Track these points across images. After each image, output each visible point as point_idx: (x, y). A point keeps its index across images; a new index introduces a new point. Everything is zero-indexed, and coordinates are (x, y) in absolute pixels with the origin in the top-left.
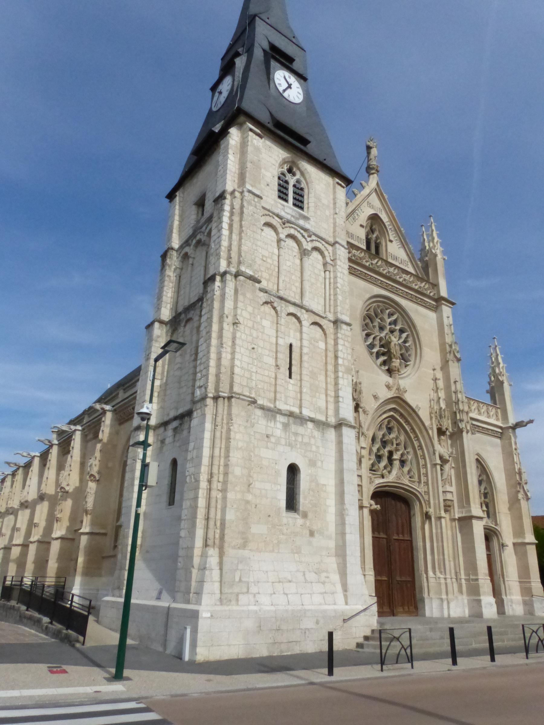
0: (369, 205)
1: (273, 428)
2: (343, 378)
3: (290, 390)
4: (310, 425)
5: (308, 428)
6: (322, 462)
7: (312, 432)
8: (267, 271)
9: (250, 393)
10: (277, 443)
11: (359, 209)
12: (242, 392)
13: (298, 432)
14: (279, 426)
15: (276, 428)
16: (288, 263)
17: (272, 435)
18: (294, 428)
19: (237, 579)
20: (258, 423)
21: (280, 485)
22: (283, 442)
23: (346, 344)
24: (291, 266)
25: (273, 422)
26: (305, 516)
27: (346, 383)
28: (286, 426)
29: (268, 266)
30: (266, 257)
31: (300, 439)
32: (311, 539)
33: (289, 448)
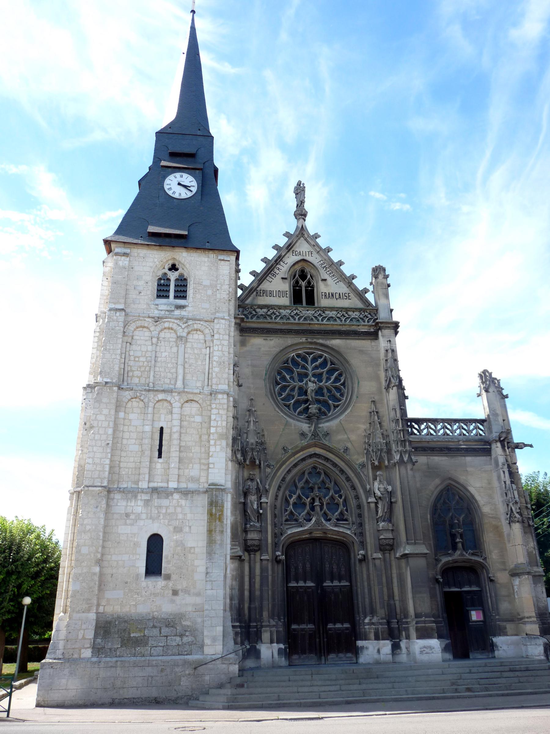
0: (294, 254)
1: (133, 506)
2: (215, 445)
3: (158, 469)
4: (176, 496)
5: (173, 499)
6: (190, 527)
7: (178, 502)
8: (139, 369)
9: (101, 483)
10: (138, 517)
11: (281, 262)
12: (93, 483)
13: (162, 505)
14: (140, 503)
15: (137, 506)
16: (164, 354)
17: (132, 513)
18: (156, 502)
19: (80, 637)
20: (117, 505)
21: (139, 554)
22: (144, 516)
23: (221, 412)
24: (168, 356)
25: (134, 501)
26: (168, 577)
27: (218, 448)
28: (147, 503)
29: (141, 364)
30: (139, 357)
31: (164, 511)
32: (175, 598)
33: (150, 521)
